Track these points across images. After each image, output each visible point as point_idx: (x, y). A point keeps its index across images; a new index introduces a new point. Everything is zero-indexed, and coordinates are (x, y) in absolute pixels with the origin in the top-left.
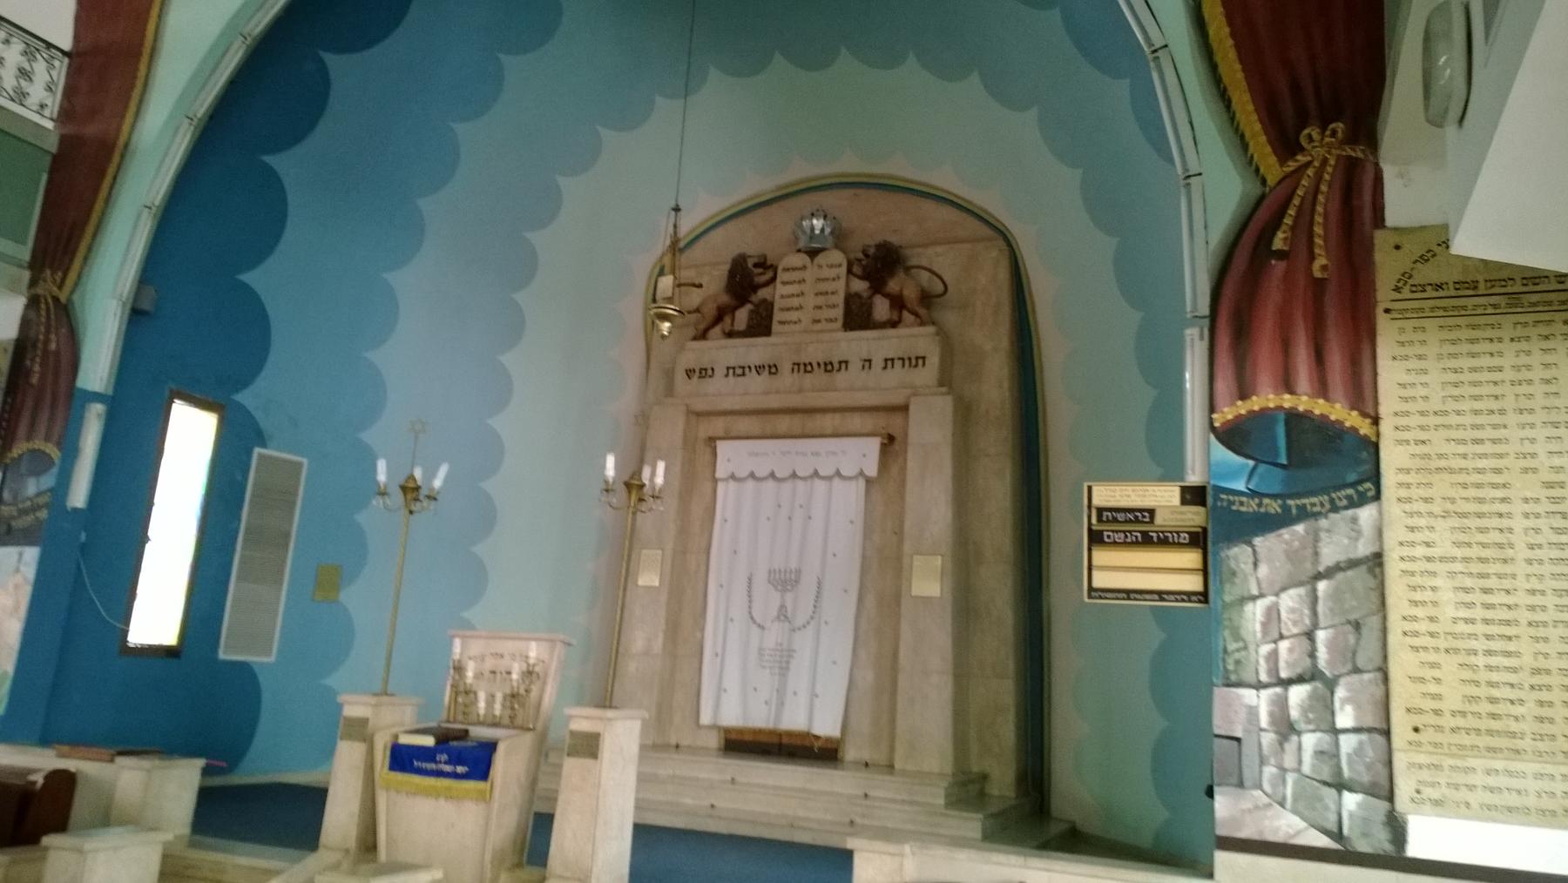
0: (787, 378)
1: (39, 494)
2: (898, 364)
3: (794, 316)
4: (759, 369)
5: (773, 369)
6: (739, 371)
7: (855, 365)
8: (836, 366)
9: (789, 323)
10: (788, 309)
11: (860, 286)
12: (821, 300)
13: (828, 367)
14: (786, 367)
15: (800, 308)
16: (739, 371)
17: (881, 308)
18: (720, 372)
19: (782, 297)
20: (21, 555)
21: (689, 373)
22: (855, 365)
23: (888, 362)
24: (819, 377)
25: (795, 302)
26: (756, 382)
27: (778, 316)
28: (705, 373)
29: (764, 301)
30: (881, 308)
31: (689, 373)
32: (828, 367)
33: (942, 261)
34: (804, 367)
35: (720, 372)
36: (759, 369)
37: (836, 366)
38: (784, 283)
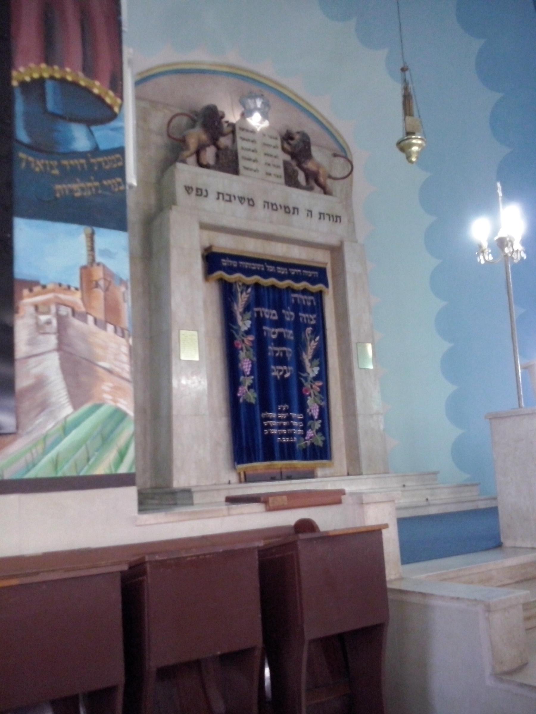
0: (261, 212)
1: (96, 151)
2: (327, 217)
3: (254, 166)
4: (241, 199)
5: (251, 202)
6: (227, 198)
7: (303, 213)
8: (292, 211)
9: (251, 170)
10: (249, 159)
11: (288, 158)
12: (269, 160)
13: (287, 210)
14: (259, 203)
15: (255, 161)
16: (227, 198)
17: (301, 177)
18: (212, 196)
19: (243, 148)
20: (91, 238)
21: (188, 189)
22: (303, 213)
23: (321, 215)
24: (280, 214)
25: (252, 155)
26: (241, 209)
27: (242, 163)
28: (200, 192)
29: (226, 148)
30: (301, 177)
31: (188, 189)
32: (287, 210)
33: (319, 157)
34: (272, 206)
35: (212, 196)
36: (241, 199)
37: (292, 211)
38: (243, 139)
